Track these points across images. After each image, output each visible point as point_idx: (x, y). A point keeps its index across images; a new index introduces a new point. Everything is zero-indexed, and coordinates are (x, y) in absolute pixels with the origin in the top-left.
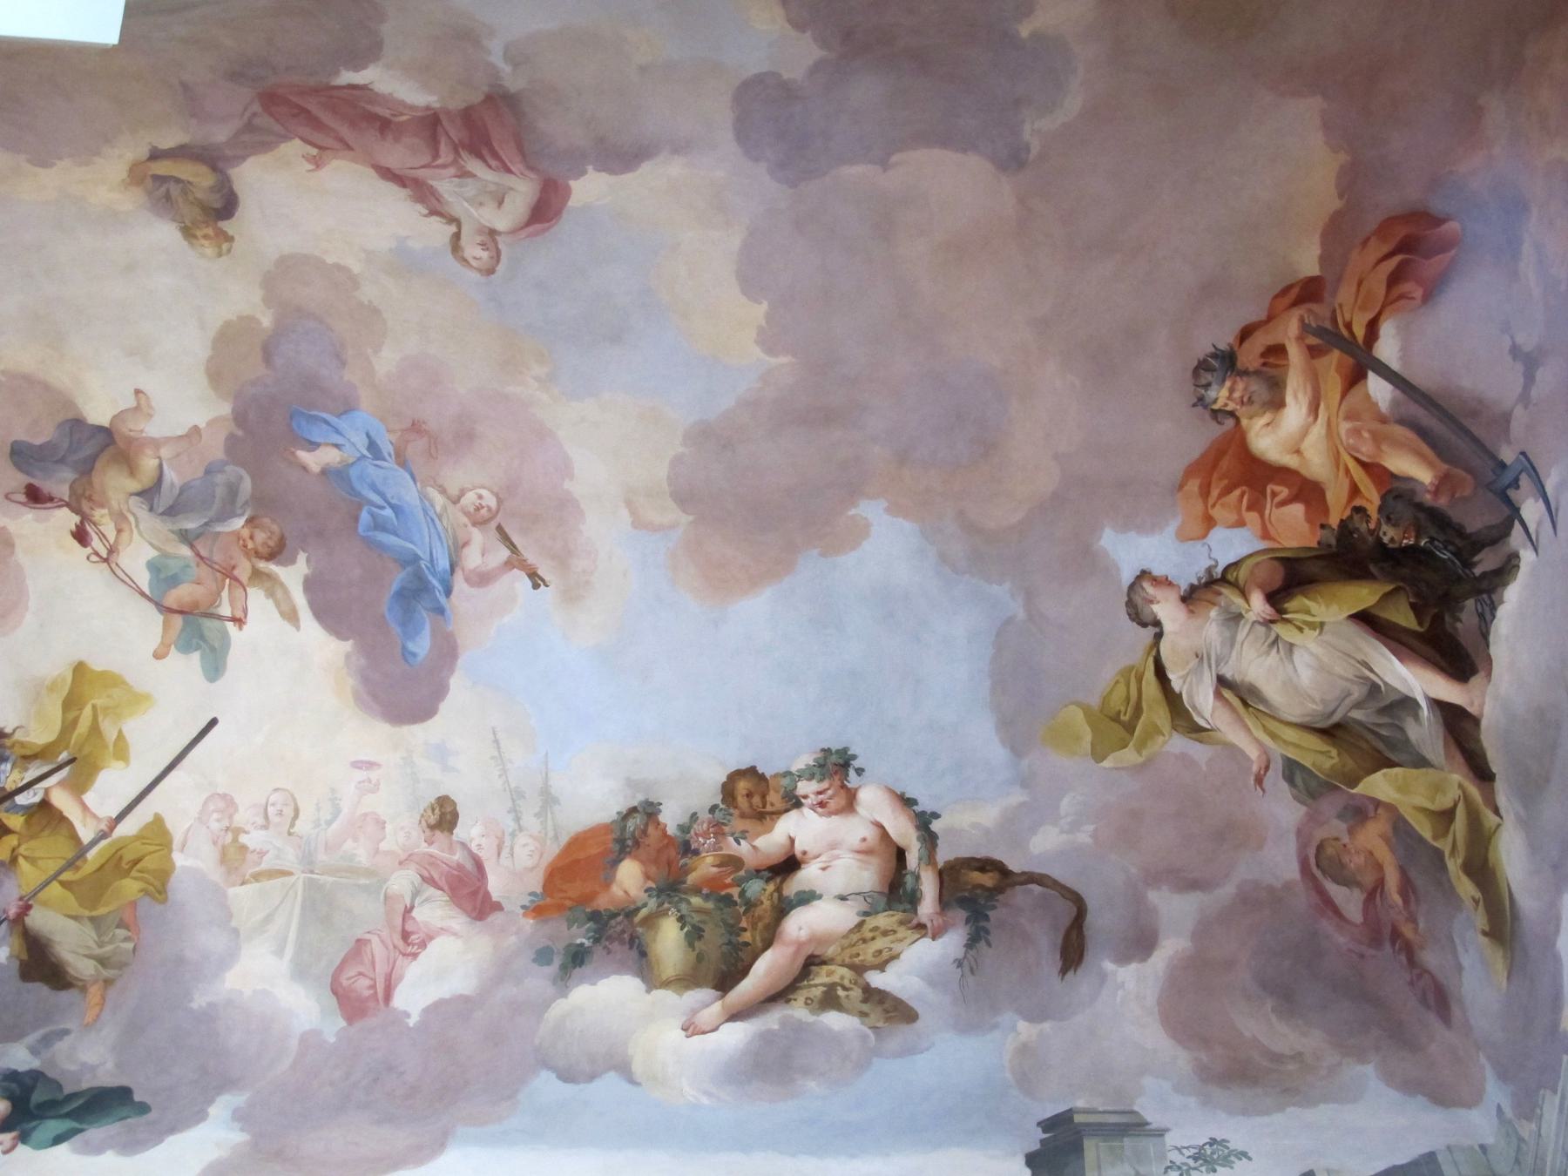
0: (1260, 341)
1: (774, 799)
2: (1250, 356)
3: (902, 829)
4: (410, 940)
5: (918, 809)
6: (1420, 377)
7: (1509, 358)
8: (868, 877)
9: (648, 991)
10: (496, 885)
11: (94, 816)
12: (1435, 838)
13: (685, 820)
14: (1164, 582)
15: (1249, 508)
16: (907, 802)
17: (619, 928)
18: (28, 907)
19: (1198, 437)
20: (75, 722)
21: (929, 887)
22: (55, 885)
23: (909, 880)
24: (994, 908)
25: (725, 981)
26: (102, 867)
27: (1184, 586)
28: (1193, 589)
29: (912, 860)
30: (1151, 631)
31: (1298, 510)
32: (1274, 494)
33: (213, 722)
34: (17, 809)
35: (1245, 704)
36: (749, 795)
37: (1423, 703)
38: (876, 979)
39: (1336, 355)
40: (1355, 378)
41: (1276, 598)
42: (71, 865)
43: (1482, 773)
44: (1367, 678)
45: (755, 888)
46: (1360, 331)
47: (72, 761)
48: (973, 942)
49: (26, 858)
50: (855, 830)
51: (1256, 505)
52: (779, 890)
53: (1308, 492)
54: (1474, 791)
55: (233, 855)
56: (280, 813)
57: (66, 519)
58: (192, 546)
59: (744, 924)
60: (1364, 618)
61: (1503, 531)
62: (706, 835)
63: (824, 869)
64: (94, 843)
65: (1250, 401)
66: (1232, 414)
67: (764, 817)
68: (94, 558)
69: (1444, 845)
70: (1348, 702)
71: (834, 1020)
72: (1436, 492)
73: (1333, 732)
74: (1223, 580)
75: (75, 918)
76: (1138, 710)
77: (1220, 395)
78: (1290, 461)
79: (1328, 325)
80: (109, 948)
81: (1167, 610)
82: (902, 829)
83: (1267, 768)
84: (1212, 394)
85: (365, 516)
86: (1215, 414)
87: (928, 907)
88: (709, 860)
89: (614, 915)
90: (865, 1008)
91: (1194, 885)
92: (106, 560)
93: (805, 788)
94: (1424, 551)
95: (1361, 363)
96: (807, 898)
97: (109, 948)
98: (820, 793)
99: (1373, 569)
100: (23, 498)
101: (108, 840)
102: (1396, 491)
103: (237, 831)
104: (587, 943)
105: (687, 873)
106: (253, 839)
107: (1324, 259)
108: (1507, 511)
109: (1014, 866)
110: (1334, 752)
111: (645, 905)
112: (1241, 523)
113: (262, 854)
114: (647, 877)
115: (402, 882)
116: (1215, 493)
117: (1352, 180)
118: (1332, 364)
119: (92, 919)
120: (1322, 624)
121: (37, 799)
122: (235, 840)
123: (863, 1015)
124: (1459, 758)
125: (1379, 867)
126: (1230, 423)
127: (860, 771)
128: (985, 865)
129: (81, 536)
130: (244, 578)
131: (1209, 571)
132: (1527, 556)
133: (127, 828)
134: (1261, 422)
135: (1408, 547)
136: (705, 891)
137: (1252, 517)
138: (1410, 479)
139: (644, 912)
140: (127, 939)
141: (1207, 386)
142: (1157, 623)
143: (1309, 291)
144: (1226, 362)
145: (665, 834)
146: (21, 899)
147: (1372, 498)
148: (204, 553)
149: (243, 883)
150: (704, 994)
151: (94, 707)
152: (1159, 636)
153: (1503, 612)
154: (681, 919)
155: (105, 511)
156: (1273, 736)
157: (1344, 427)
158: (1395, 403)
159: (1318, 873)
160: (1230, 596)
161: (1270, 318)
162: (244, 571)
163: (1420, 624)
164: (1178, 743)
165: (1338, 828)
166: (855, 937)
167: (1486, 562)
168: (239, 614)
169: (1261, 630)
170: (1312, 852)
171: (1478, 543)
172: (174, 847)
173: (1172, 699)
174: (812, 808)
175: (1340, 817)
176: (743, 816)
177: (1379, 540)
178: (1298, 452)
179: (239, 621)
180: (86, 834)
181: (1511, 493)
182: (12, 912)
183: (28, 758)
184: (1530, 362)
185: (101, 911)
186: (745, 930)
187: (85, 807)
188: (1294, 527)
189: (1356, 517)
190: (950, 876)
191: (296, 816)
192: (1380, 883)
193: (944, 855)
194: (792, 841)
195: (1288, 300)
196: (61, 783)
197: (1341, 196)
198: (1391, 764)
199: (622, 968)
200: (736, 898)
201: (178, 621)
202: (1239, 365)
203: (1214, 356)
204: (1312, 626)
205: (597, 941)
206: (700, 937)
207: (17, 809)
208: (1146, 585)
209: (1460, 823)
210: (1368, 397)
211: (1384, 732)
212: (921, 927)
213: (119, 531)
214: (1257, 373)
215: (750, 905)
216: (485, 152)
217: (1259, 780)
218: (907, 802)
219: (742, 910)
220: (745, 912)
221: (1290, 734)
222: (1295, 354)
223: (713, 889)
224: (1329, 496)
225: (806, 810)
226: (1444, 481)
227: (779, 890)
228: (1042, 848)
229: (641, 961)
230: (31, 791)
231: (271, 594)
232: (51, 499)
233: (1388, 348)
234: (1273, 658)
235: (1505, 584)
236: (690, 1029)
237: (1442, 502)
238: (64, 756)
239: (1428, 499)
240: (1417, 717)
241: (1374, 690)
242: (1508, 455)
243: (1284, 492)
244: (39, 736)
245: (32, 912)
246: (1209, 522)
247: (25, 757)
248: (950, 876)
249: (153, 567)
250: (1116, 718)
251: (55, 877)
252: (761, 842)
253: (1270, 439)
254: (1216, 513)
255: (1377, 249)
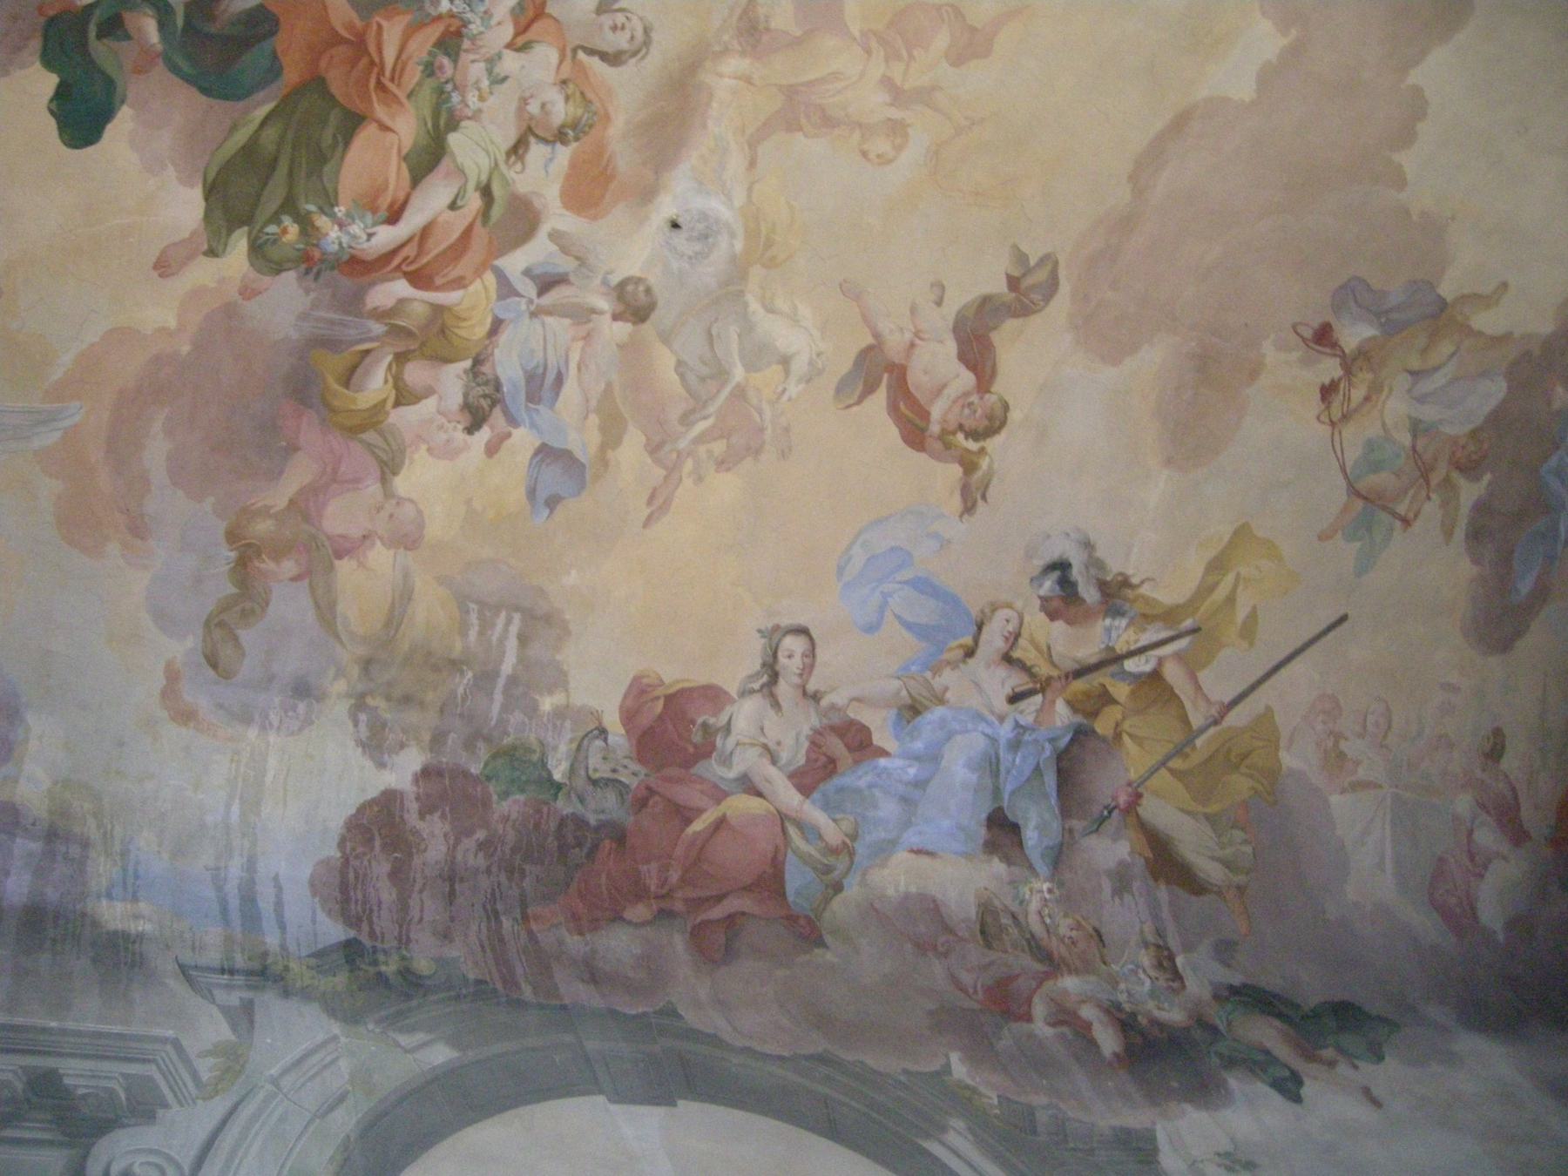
4: (1478, 863)
10: (1527, 813)
11: (1208, 700)
18: (1139, 796)
20: (1213, 588)
22: (1163, 771)
26: (1211, 757)
33: (1343, 619)
34: (1124, 676)
42: (1179, 752)
47: (1194, 631)
49: (1130, 736)
55: (1336, 760)
56: (1377, 725)
57: (1330, 369)
58: (1415, 436)
64: (1202, 730)
68: (1324, 418)
75: (1188, 813)
80: (1228, 851)
85: (1553, 462)
92: (1333, 424)
97: (1228, 851)
100: (1308, 333)
101: (1218, 728)
103: (1338, 737)
106: (1352, 747)
113: (1357, 763)
115: (1463, 803)
119: (1207, 817)
121: (1148, 668)
122: (1336, 743)
129: (1327, 391)
130: (1434, 482)
133: (1235, 718)
140: (1246, 842)
146: (1130, 784)
148: (1419, 448)
149: (1343, 791)
151: (1238, 574)
155: (1370, 376)
162: (1435, 479)
168: (1411, 515)
172: (1282, 744)
179: (1406, 522)
180: (1196, 721)
182: (1123, 799)
183: (1147, 618)
185: (1213, 808)
187: (1198, 687)
191: (1389, 727)
196: (1178, 656)
201: (1359, 504)
207: (1124, 676)
213: (1367, 399)
230: (1143, 658)
231: (1445, 504)
232: (1334, 345)
238: (1188, 623)
244: (1169, 593)
245: (1144, 801)
247: (1145, 616)
249: (1370, 446)
251: (1163, 764)
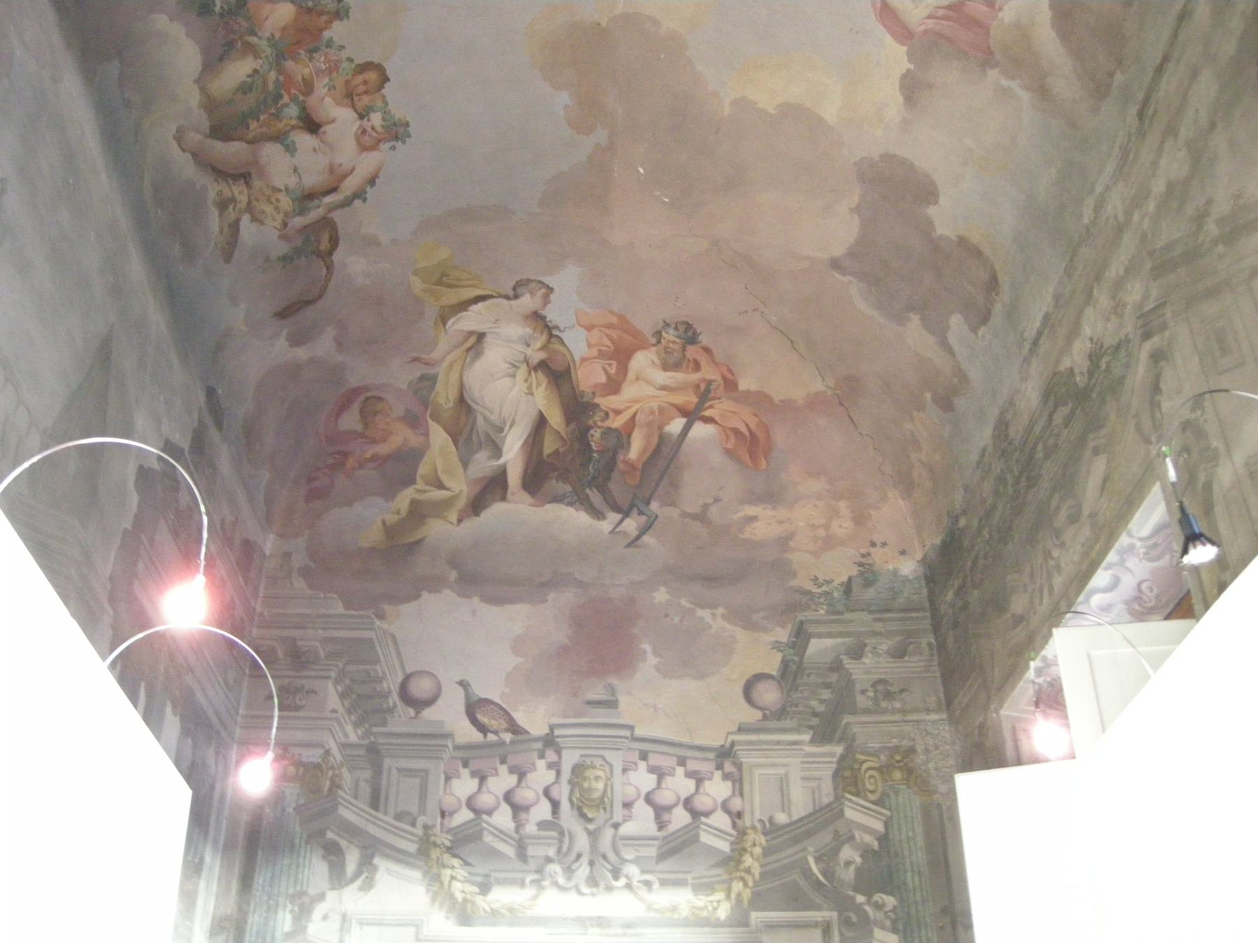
0: (703, 360)
1: (366, 100)
2: (692, 352)
3: (349, 186)
5: (369, 189)
6: (685, 447)
7: (701, 502)
8: (312, 179)
9: (197, 81)
12: (422, 477)
13: (338, 41)
14: (546, 300)
15: (600, 351)
16: (372, 181)
17: (236, 27)
19: (645, 324)
21: (314, 215)
23: (316, 202)
24: (307, 257)
25: (220, 131)
27: (544, 313)
28: (543, 318)
29: (328, 199)
30: (511, 293)
31: (603, 379)
32: (610, 365)
35: (469, 350)
36: (365, 82)
37: (501, 461)
38: (245, 220)
39: (695, 400)
40: (684, 412)
41: (543, 366)
43: (477, 505)
44: (505, 423)
45: (293, 111)
46: (707, 413)
48: (286, 259)
50: (347, 152)
51: (601, 355)
52: (293, 128)
53: (614, 386)
54: (462, 503)
59: (262, 118)
60: (541, 423)
61: (617, 509)
62: (327, 61)
63: (314, 150)
65: (667, 353)
66: (659, 342)
67: (349, 96)
69: (420, 485)
70: (487, 413)
71: (214, 221)
72: (625, 462)
73: (462, 401)
74: (551, 335)
76: (450, 286)
77: (670, 336)
78: (631, 375)
79: (712, 394)
81: (527, 302)
82: (349, 186)
83: (427, 364)
84: (671, 331)
86: (658, 334)
87: (298, 221)
88: (307, 71)
89: (248, 19)
90: (226, 230)
91: (339, 344)
93: (376, 119)
94: (590, 458)
95: (692, 415)
96: (291, 149)
98: (373, 128)
99: (573, 426)
102: (621, 438)
104: (217, 9)
105: (293, 59)
107: (748, 393)
108: (625, 507)
109: (337, 257)
110: (451, 405)
111: (260, 38)
112: (590, 346)
114: (284, 29)
116: (609, 332)
117: (787, 406)
118: (691, 399)
120: (532, 394)
123: (221, 231)
124: (477, 489)
125: (384, 440)
126: (654, 341)
127: (393, 148)
128: (334, 242)
131: (557, 327)
132: (605, 526)
134: (654, 357)
135: (590, 446)
136: (281, 78)
137: (595, 352)
138: (629, 444)
139: (254, 40)
141: (676, 328)
142: (516, 297)
143: (730, 385)
144: (690, 335)
145: (321, 31)
147: (617, 423)
150: (205, 124)
152: (507, 297)
153: (571, 510)
154: (256, 71)
156: (451, 366)
157: (655, 405)
158: (670, 435)
159: (363, 397)
160: (540, 341)
161: (716, 363)
163: (548, 456)
164: (431, 313)
165: (399, 410)
166: (269, 192)
167: (595, 497)
169: (522, 358)
170: (376, 393)
171: (603, 490)
173: (464, 305)
174: (361, 126)
175: (407, 410)
176: (347, 83)
177: (592, 427)
178: (638, 379)
181: (635, 511)
184: (701, 517)
186: (258, 120)
188: (589, 377)
189: (602, 414)
190: (326, 223)
192: (374, 441)
193: (337, 216)
194: (333, 121)
195: (726, 373)
197: (781, 401)
198: (456, 444)
199: (206, 52)
200: (281, 102)
202: (688, 347)
203: (694, 333)
204: (530, 388)
205: (222, 15)
206: (245, 93)
208: (543, 290)
209: (443, 494)
210: (672, 418)
211: (474, 437)
212: (285, 225)
214: (684, 356)
215: (277, 116)
216: (951, 13)
217: (415, 360)
218: (372, 181)
219: (273, 111)
220: (272, 115)
221: (454, 377)
222: (696, 377)
223: (286, 83)
224: (613, 398)
225: (358, 123)
226: (631, 466)
227: (293, 128)
228: (353, 264)
229: (213, 62)
233: (700, 431)
234: (504, 366)
235: (586, 511)
236: (179, 137)
237: (620, 465)
239: (621, 457)
240: (490, 458)
241: (501, 430)
242: (654, 506)
243: (613, 371)
246: (589, 328)
248: (326, 223)
250: (444, 275)
252: (328, 100)
253: (643, 361)
254: (596, 331)
255: (752, 421)
